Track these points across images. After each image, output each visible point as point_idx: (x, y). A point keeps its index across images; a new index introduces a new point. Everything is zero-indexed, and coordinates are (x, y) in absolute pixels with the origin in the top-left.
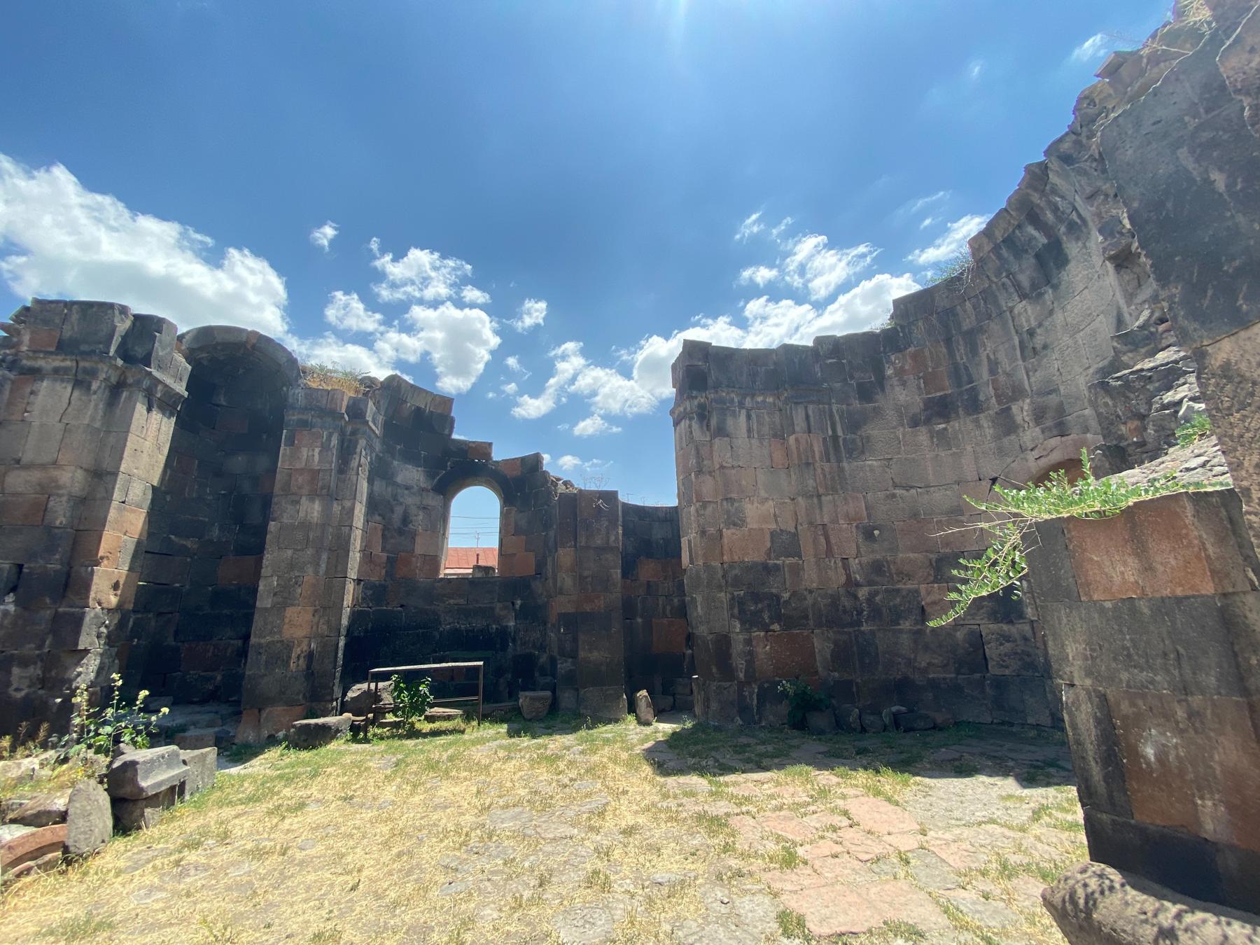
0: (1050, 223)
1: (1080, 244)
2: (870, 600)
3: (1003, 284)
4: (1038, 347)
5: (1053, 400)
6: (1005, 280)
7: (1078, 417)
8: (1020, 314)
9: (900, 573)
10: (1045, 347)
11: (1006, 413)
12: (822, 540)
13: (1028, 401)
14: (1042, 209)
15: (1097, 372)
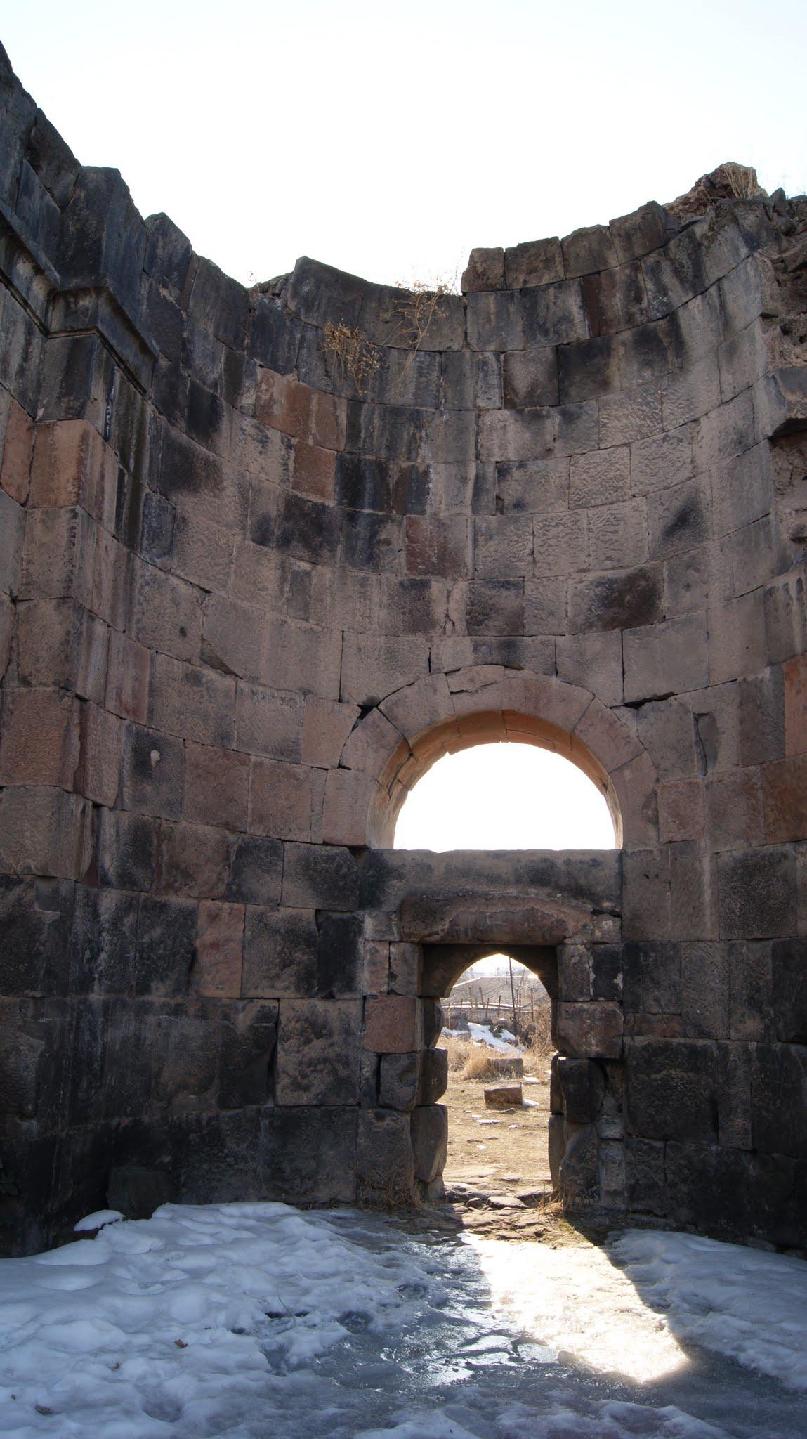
0: (610, 315)
1: (647, 374)
2: (116, 922)
3: (485, 363)
4: (508, 500)
5: (508, 600)
6: (489, 356)
7: (542, 643)
8: (492, 429)
9: (174, 866)
10: (519, 505)
11: (418, 588)
12: (76, 743)
13: (463, 585)
14: (613, 284)
15: (599, 584)
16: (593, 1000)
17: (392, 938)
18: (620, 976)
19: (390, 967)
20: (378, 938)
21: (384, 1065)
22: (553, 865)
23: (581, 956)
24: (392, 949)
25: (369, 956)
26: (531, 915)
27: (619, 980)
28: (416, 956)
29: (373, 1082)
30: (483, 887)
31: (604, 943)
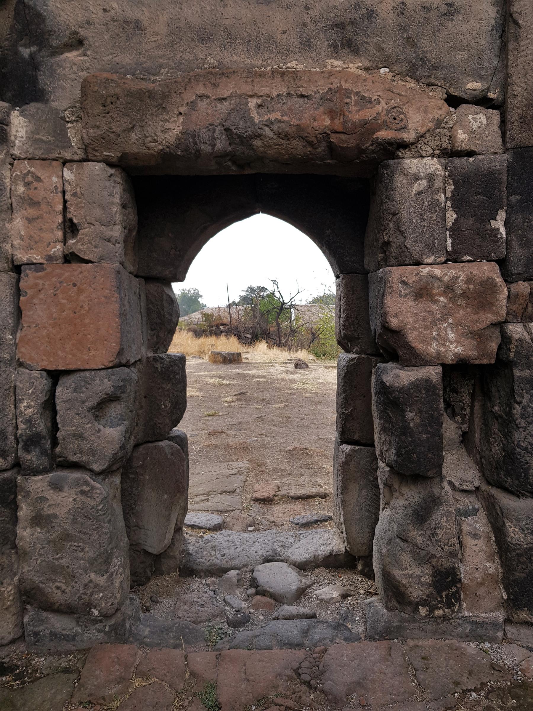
16: (454, 258)
17: (68, 155)
18: (502, 215)
19: (65, 208)
20: (39, 153)
21: (62, 392)
22: (371, 14)
23: (431, 178)
24: (68, 174)
25: (21, 189)
26: (335, 101)
27: (499, 224)
28: (118, 189)
29: (42, 426)
30: (238, 58)
31: (470, 154)
